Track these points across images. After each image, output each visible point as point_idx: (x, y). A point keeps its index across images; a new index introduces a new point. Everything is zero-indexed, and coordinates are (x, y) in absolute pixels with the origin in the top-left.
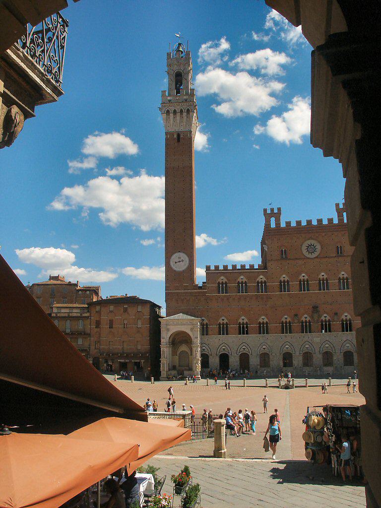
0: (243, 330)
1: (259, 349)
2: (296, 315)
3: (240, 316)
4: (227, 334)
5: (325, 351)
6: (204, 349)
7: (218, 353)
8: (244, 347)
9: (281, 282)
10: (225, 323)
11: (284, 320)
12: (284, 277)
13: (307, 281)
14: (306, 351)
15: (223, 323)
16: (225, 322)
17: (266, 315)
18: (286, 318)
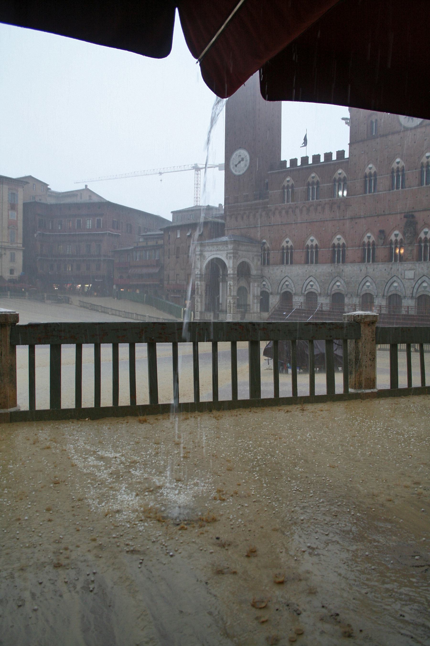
0: (311, 256)
1: (331, 286)
2: (382, 232)
3: (308, 236)
4: (291, 263)
5: (421, 293)
6: (264, 285)
7: (279, 290)
8: (311, 283)
9: (366, 177)
10: (289, 246)
11: (366, 240)
12: (371, 168)
13: (403, 170)
14: (394, 292)
15: (287, 246)
16: (290, 244)
17: (343, 234)
18: (370, 237)
